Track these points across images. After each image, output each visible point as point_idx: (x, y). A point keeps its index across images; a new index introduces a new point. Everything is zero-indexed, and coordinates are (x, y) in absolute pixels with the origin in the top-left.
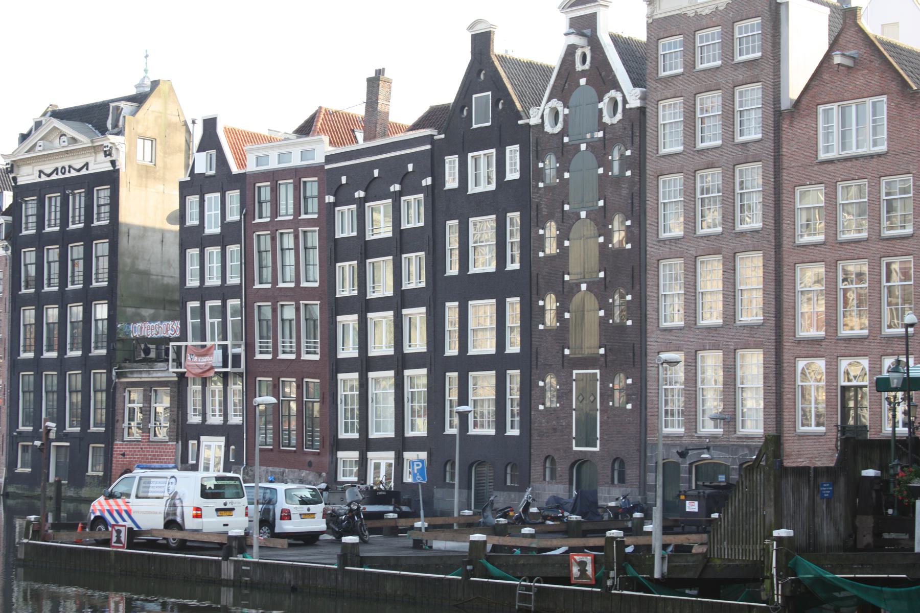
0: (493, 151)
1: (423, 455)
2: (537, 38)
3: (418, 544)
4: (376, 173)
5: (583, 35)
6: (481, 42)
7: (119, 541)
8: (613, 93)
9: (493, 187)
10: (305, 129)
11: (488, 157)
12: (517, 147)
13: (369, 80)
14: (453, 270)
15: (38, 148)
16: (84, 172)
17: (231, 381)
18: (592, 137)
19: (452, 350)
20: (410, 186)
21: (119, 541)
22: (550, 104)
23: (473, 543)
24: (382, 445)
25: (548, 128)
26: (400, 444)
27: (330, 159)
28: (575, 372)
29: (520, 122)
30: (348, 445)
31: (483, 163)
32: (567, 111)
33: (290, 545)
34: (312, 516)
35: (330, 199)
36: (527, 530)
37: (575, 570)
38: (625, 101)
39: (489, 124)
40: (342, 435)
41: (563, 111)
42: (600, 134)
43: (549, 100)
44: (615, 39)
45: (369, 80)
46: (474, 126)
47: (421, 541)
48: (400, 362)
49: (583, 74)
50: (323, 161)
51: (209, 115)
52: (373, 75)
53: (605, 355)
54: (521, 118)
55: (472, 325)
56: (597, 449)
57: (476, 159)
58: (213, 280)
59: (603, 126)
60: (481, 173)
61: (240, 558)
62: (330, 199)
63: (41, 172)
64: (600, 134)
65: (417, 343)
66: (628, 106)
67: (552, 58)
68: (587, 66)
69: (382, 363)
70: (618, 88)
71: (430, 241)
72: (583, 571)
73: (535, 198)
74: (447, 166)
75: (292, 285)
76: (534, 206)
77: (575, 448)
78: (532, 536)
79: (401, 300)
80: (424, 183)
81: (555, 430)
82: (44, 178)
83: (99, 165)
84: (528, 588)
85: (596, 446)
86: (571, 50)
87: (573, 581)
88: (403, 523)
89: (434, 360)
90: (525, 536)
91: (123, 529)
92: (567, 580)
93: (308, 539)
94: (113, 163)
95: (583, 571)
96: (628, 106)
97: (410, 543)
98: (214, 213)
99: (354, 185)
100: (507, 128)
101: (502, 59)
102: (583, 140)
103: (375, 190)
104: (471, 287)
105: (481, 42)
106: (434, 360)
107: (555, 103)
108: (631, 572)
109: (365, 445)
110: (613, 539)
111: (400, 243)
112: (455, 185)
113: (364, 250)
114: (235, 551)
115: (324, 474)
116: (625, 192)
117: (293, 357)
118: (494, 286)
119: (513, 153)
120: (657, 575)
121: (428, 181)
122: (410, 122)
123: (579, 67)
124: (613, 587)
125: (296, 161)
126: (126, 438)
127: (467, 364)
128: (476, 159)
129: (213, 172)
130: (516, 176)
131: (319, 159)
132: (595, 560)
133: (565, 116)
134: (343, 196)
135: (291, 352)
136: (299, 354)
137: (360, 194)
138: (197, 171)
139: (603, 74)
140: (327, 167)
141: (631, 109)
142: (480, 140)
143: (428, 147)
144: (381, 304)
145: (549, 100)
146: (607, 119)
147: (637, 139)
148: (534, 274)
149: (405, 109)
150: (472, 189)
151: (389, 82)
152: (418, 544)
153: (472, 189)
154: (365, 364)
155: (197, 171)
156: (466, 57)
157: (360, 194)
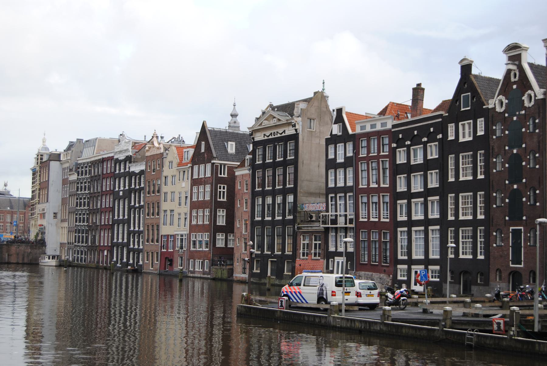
0: (471, 121)
1: (437, 268)
2: (492, 67)
3: (425, 311)
4: (416, 132)
5: (515, 64)
6: (466, 69)
7: (282, 306)
8: (529, 92)
9: (471, 139)
10: (383, 113)
11: (469, 124)
12: (483, 119)
13: (414, 89)
14: (451, 179)
15: (263, 124)
16: (283, 135)
17: (339, 232)
18: (519, 114)
19: (451, 218)
20: (432, 138)
21: (282, 306)
22: (498, 98)
23: (445, 311)
24: (418, 262)
25: (498, 109)
26: (427, 262)
27: (394, 126)
28: (511, 228)
29: (484, 107)
30: (403, 262)
31: (467, 127)
32: (507, 101)
33: (360, 310)
34: (372, 295)
35: (394, 145)
36: (478, 305)
37: (495, 327)
38: (535, 96)
39: (469, 108)
40: (400, 257)
41: (505, 101)
42: (523, 112)
43: (498, 96)
44: (531, 65)
45: (414, 89)
46: (462, 109)
47: (426, 309)
48: (427, 222)
49: (515, 83)
50: (391, 127)
51: (339, 106)
52: (415, 86)
53: (526, 220)
54: (485, 105)
55: (325, 204)
56: (522, 266)
57: (463, 125)
58: (341, 184)
59: (525, 108)
61: (336, 316)
62: (394, 145)
63: (264, 135)
64: (523, 112)
65: (435, 215)
66: (537, 98)
67: (499, 75)
69: (418, 223)
70: (532, 89)
71: (440, 165)
72: (499, 327)
73: (491, 143)
75: (366, 186)
76: (491, 147)
77: (511, 266)
78: (480, 308)
79: (427, 192)
80: (438, 137)
81: (501, 256)
82: (266, 138)
83: (290, 131)
84: (472, 335)
85: (521, 264)
86: (509, 72)
87: (494, 332)
88: (420, 300)
89: (442, 221)
90: (476, 308)
91: (283, 300)
92: (491, 332)
93: (372, 307)
94: (296, 130)
95: (499, 327)
96: (537, 98)
97: (421, 311)
98: (341, 153)
99: (404, 139)
100: (478, 110)
101: (476, 76)
102: (515, 115)
103: (416, 141)
104: (460, 187)
105: (466, 69)
106: (442, 221)
107: (501, 97)
108: (524, 328)
109: (410, 262)
110: (514, 311)
111: (427, 166)
112: (453, 138)
113: (409, 169)
114: (333, 312)
115: (391, 276)
116: (535, 140)
117: (366, 220)
118: (472, 186)
119: (481, 122)
120: (536, 330)
121: (440, 136)
122: (433, 108)
123: (513, 79)
124: (514, 335)
125: (379, 128)
126: (301, 257)
127: (458, 224)
128: (463, 125)
129: (341, 134)
130: (483, 133)
131: (389, 126)
132: (505, 323)
133: (506, 103)
135: (365, 218)
136: (369, 218)
137: (408, 143)
138: (333, 133)
139: (525, 83)
140: (393, 130)
141: (538, 99)
142: (465, 116)
143: (440, 120)
144: (418, 195)
145: (498, 96)
146: (527, 104)
147: (541, 114)
148: (491, 180)
149: (431, 102)
150: (461, 140)
151: (423, 89)
152: (425, 311)
153: (461, 140)
154: (410, 223)
155: (333, 133)
156: (459, 77)
157: (408, 143)
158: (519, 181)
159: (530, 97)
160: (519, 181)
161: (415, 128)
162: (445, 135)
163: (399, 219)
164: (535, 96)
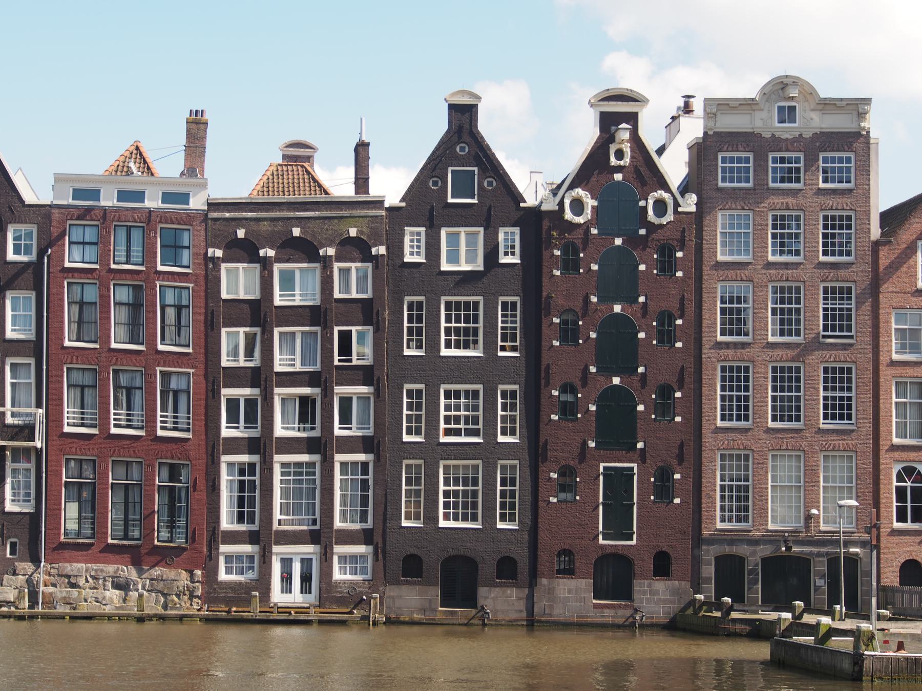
6: (463, 115)
25: (568, 215)
32: (596, 203)
41: (590, 203)
43: (571, 187)
49: (619, 169)
50: (206, 208)
60: (461, 252)
68: (627, 161)
74: (407, 239)
96: (680, 209)
105: (463, 115)
107: (579, 192)
112: (421, 259)
123: (613, 161)
133: (593, 207)
134: (245, 251)
142: (461, 216)
158: (628, 370)
159: (660, 207)
160: (628, 370)
161: (300, 221)
162: (396, 248)
163: (226, 432)
164: (677, 205)
